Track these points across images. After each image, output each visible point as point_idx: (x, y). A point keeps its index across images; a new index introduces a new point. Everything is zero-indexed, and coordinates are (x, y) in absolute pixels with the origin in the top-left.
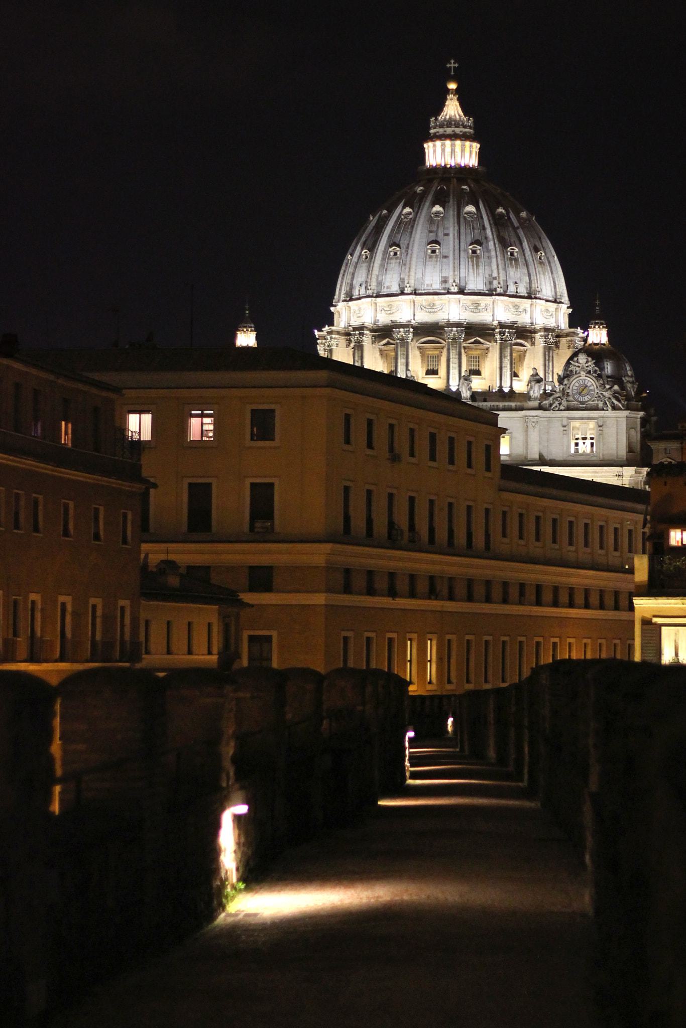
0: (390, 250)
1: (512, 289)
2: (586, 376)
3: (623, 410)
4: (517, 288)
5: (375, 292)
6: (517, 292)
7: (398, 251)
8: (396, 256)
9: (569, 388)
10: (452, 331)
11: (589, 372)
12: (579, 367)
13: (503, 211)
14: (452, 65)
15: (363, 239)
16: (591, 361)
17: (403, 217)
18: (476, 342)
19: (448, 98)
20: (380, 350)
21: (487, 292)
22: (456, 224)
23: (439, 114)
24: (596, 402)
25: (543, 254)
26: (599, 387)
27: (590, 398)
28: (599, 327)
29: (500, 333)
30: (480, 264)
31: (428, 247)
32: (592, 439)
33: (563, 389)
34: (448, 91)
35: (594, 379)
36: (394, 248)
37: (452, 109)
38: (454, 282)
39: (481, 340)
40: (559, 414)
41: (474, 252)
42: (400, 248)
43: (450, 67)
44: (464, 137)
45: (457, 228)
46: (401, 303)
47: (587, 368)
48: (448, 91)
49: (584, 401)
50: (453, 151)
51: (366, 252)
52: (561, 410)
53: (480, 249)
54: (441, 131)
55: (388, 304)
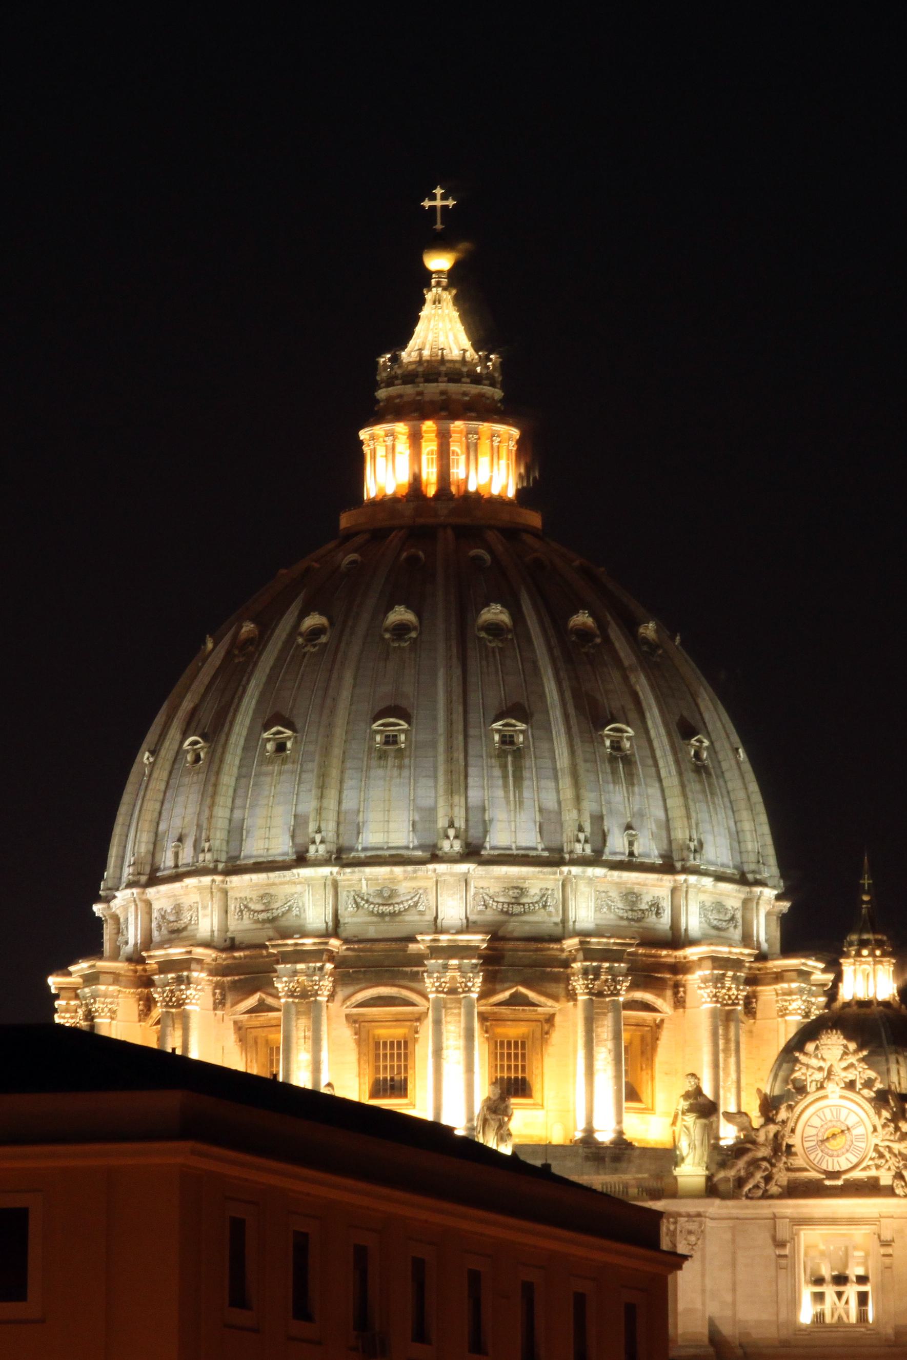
0: (266, 735)
1: (617, 844)
2: (842, 1097)
4: (631, 844)
5: (223, 857)
6: (631, 854)
7: (289, 738)
8: (283, 754)
9: (793, 1131)
10: (446, 967)
11: (851, 1085)
12: (820, 1069)
13: (590, 621)
14: (438, 203)
15: (187, 705)
16: (856, 1052)
17: (300, 640)
18: (517, 1001)
19: (429, 296)
20: (239, 1027)
21: (546, 854)
22: (455, 661)
23: (403, 345)
24: (873, 1173)
25: (706, 743)
26: (879, 1128)
27: (855, 1160)
28: (872, 954)
29: (585, 972)
30: (526, 774)
31: (375, 727)
32: (862, 1280)
35: (868, 1106)
36: (274, 729)
38: (451, 825)
39: (532, 995)
40: (766, 1208)
41: (507, 740)
42: (294, 730)
43: (433, 208)
46: (299, 888)
49: (837, 1168)
51: (195, 743)
52: (772, 1197)
53: (522, 732)
55: (262, 892)
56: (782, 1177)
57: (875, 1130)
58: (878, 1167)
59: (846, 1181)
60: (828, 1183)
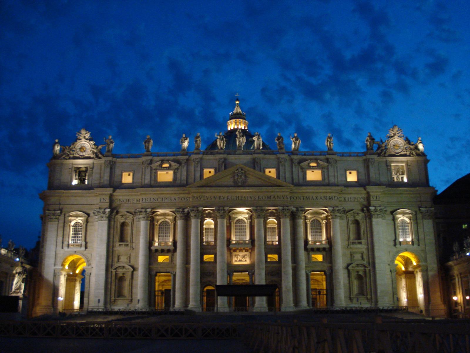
2: (398, 139)
9: (389, 145)
11: (399, 137)
24: (405, 153)
27: (401, 150)
35: (403, 140)
40: (384, 159)
47: (398, 135)
48: (235, 104)
49: (398, 152)
52: (386, 156)
56: (388, 153)
57: (405, 145)
58: (406, 151)
60: (397, 154)
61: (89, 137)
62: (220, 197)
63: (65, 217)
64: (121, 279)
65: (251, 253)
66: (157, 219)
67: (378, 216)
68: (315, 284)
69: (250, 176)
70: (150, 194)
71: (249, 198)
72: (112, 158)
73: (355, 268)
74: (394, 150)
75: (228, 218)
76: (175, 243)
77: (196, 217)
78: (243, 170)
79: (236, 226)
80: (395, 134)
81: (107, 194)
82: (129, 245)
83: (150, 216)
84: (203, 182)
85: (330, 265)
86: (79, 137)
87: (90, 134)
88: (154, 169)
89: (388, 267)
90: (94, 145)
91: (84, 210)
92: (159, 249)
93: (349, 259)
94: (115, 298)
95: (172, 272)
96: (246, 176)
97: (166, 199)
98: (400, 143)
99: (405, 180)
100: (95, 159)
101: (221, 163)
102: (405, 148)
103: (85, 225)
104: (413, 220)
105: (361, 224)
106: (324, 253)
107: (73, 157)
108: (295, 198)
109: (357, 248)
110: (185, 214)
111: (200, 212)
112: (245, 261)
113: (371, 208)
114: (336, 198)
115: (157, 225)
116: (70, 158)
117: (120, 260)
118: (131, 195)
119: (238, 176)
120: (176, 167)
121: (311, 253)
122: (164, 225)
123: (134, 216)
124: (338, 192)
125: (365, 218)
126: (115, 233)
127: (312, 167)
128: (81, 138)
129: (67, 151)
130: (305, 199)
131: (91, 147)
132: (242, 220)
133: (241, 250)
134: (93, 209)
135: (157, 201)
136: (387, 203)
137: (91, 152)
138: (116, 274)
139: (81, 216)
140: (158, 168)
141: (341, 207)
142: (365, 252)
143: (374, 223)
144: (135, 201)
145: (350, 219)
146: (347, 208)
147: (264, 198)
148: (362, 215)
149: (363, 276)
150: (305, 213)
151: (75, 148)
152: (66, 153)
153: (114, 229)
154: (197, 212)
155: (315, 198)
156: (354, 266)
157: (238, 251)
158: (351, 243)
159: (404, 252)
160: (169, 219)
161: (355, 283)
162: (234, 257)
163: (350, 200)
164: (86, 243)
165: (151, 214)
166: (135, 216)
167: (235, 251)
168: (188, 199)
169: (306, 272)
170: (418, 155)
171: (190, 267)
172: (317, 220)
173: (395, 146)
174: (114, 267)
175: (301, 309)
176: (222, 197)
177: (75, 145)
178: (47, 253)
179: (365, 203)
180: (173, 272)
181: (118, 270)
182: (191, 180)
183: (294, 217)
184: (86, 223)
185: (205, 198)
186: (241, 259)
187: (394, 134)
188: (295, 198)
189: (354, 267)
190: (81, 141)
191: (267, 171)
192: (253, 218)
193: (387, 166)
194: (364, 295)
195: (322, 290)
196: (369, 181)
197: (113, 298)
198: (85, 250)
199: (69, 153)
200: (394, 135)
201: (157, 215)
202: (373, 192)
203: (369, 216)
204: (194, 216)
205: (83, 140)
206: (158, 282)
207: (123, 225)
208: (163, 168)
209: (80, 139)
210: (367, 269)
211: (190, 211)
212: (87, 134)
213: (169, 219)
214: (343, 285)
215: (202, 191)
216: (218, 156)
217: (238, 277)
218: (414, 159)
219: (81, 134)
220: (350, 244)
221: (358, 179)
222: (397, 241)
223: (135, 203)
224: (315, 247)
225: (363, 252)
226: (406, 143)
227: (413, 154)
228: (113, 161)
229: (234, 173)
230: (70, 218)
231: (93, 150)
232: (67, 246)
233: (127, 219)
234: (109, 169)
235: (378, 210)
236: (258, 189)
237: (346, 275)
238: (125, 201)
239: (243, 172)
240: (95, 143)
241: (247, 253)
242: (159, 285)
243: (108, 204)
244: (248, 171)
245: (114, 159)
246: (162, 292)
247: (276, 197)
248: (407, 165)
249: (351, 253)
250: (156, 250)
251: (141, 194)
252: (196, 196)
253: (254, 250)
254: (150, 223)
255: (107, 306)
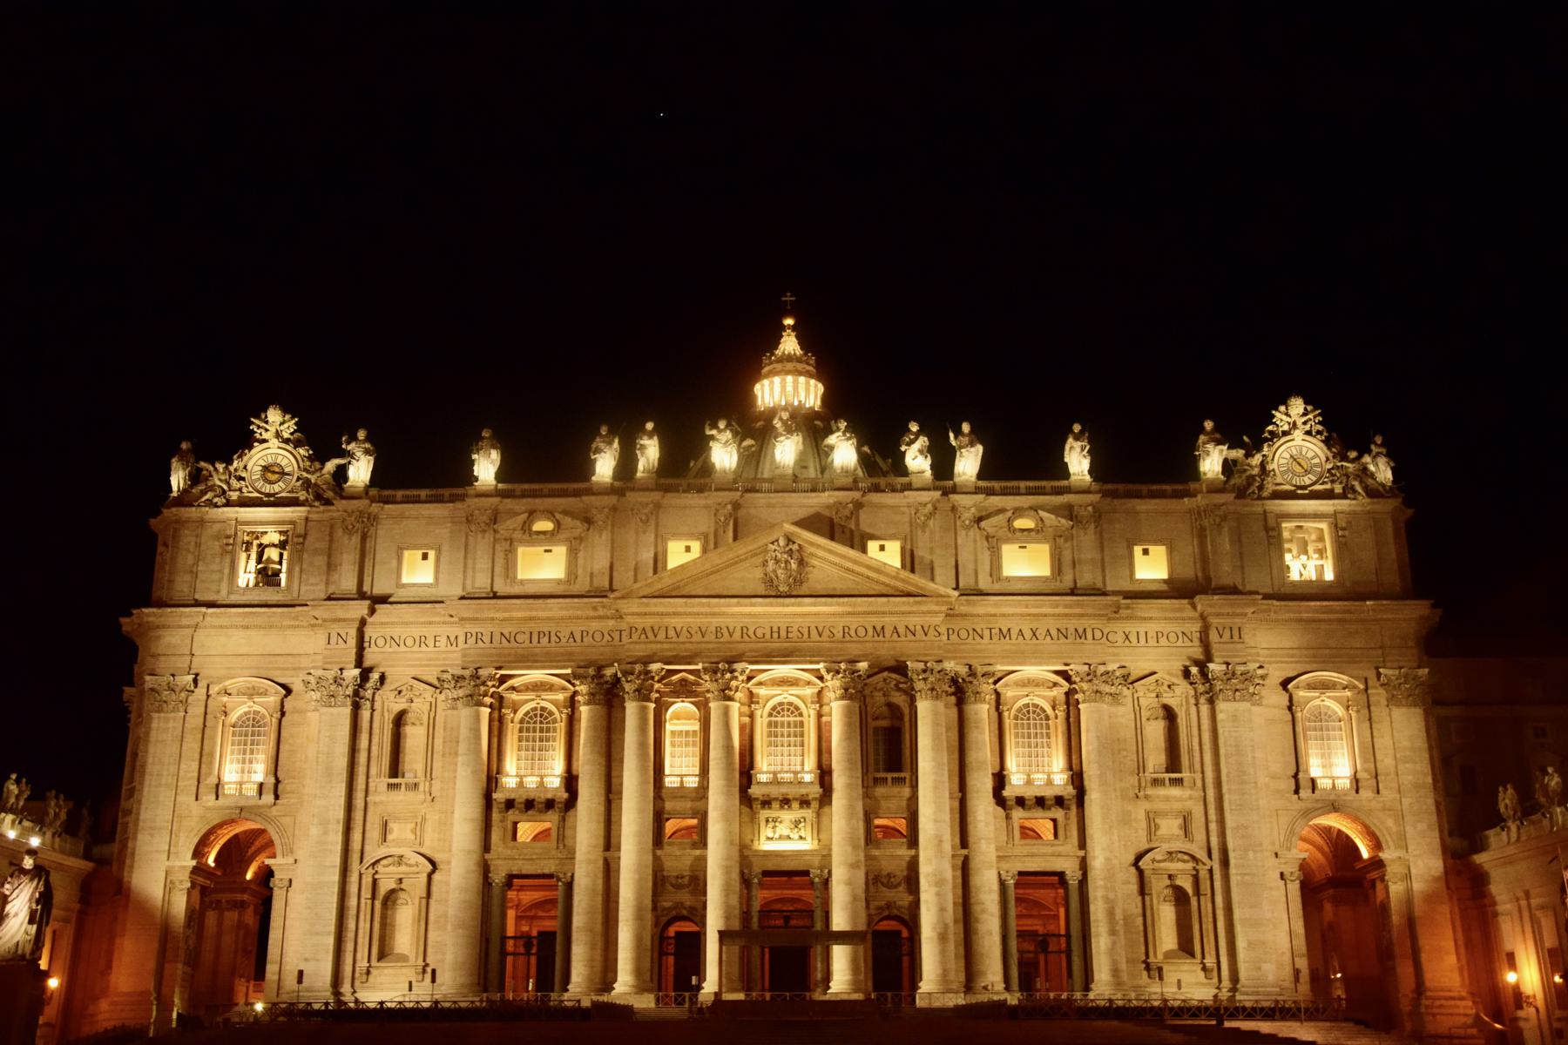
3: (1388, 497)
9: (1273, 460)
11: (1308, 433)
16: (1312, 411)
24: (1328, 486)
27: (1314, 479)
33: (1263, 461)
34: (783, 328)
35: (1322, 445)
37: (790, 344)
40: (1258, 507)
44: (809, 375)
45: (817, 460)
50: (796, 388)
52: (1264, 498)
54: (779, 366)
56: (1270, 487)
57: (1328, 459)
58: (1333, 482)
59: (1311, 491)
60: (1299, 492)
61: (292, 434)
62: (718, 630)
63: (208, 696)
64: (390, 899)
65: (818, 815)
66: (514, 702)
67: (1237, 693)
68: (1031, 916)
69: (814, 562)
70: (493, 619)
71: (814, 632)
72: (367, 501)
73: (1162, 865)
74: (1292, 478)
75: (745, 700)
76: (570, 781)
77: (642, 695)
78: (794, 543)
79: (770, 724)
80: (1294, 426)
81: (353, 620)
82: (421, 788)
83: (492, 690)
84: (665, 582)
85: (1082, 853)
86: (261, 434)
87: (296, 424)
88: (506, 540)
89: (1272, 861)
90: (310, 458)
91: (271, 674)
92: (521, 797)
93: (1143, 834)
94: (369, 961)
95: (561, 875)
96: (801, 562)
97: (542, 635)
98: (1310, 454)
99: (1329, 576)
100: (311, 506)
101: (722, 519)
102: (1329, 470)
103: (275, 721)
104: (1355, 708)
105: (1179, 720)
106: (1058, 814)
107: (239, 497)
108: (964, 634)
109: (1167, 799)
110: (606, 686)
111: (653, 678)
112: (801, 838)
113: (1211, 666)
114: (1098, 634)
115: (512, 722)
116: (228, 504)
117: (389, 837)
118: (430, 623)
119: (777, 561)
120: (577, 532)
121: (1018, 814)
122: (535, 722)
123: (438, 691)
124: (1103, 615)
125: (1193, 701)
126: (374, 748)
127: (1019, 534)
128: (265, 436)
129: (220, 480)
130: (995, 639)
131: (299, 467)
132: (790, 704)
133: (785, 802)
134: (300, 668)
135: (513, 644)
136: (1266, 652)
137: (300, 482)
138: (375, 882)
139: (265, 693)
140: (517, 535)
141: (1114, 661)
142: (1198, 811)
143: (1220, 716)
144: (443, 641)
145: (1143, 702)
146: (1137, 669)
147: (861, 632)
148: (1183, 687)
149: (1190, 891)
150: (995, 683)
151: (245, 467)
152: (214, 485)
153: (371, 734)
154: (642, 677)
155: (1028, 634)
156: (1159, 857)
157: (776, 805)
158: (1149, 785)
159: (1329, 812)
160: (552, 701)
161: (1166, 915)
162: (763, 824)
163: (1142, 639)
164: (278, 781)
165: (493, 686)
166: (441, 693)
167: (766, 803)
168: (616, 635)
169: (999, 874)
170: (1372, 493)
171: (619, 858)
172: (1036, 706)
173: (1295, 460)
174: (368, 860)
175: (983, 998)
176: (725, 631)
177: (245, 458)
178: (142, 816)
179: (1197, 653)
180: (565, 874)
181: (379, 868)
182: (624, 578)
183: (960, 692)
184: (278, 715)
185: (672, 633)
186: (786, 832)
187: (1289, 424)
188: (964, 634)
189: (1159, 861)
190: (265, 445)
191: (872, 546)
192: (825, 700)
193: (1267, 529)
194: (1192, 955)
195: (1053, 935)
196: (1208, 579)
197: (362, 964)
198: (275, 804)
199: (225, 487)
200: (1290, 430)
201: (513, 688)
202: (1218, 615)
203: (1208, 693)
204: (635, 691)
205: (274, 442)
206: (517, 906)
207: (399, 720)
208: (535, 537)
209: (265, 441)
210: (1203, 874)
211: (619, 675)
212: (286, 425)
213: (552, 702)
214: (1121, 922)
215: (661, 609)
216: (713, 498)
217: (779, 892)
218: (1360, 509)
219: (267, 422)
220: (1143, 784)
221: (1171, 573)
222: (1301, 775)
223: (443, 648)
224: (1029, 793)
225: (1190, 813)
226: (1330, 455)
227: (1354, 491)
228: (369, 514)
229: (766, 551)
230: (225, 699)
231: (305, 474)
232: (214, 790)
233: (415, 700)
234: (356, 540)
235: (1239, 673)
236: (843, 604)
237: (1134, 887)
238: (410, 642)
239: (795, 547)
240: (311, 452)
241: (808, 813)
242: (518, 918)
243: (354, 651)
244: (812, 544)
245: (375, 507)
246: (526, 939)
247: (901, 630)
248: (1335, 527)
249: (1148, 813)
250: (510, 804)
251: (462, 619)
252: (640, 627)
253: (830, 803)
254: (490, 713)
255: (342, 990)
